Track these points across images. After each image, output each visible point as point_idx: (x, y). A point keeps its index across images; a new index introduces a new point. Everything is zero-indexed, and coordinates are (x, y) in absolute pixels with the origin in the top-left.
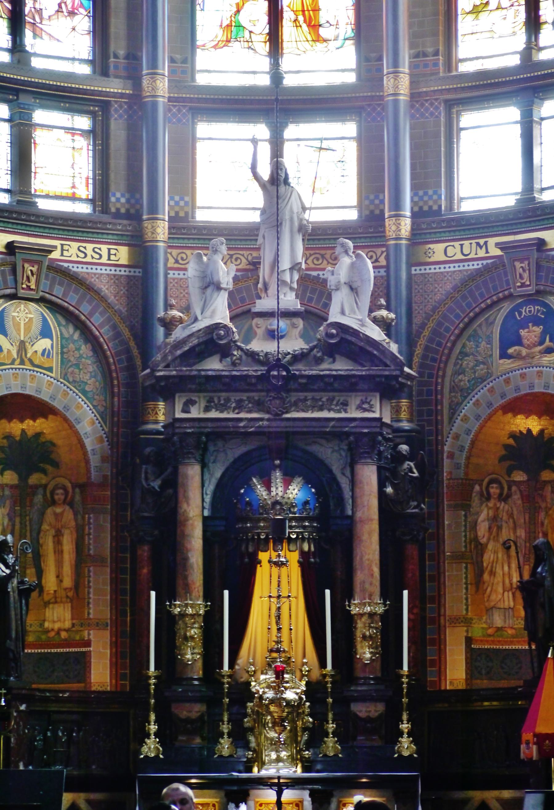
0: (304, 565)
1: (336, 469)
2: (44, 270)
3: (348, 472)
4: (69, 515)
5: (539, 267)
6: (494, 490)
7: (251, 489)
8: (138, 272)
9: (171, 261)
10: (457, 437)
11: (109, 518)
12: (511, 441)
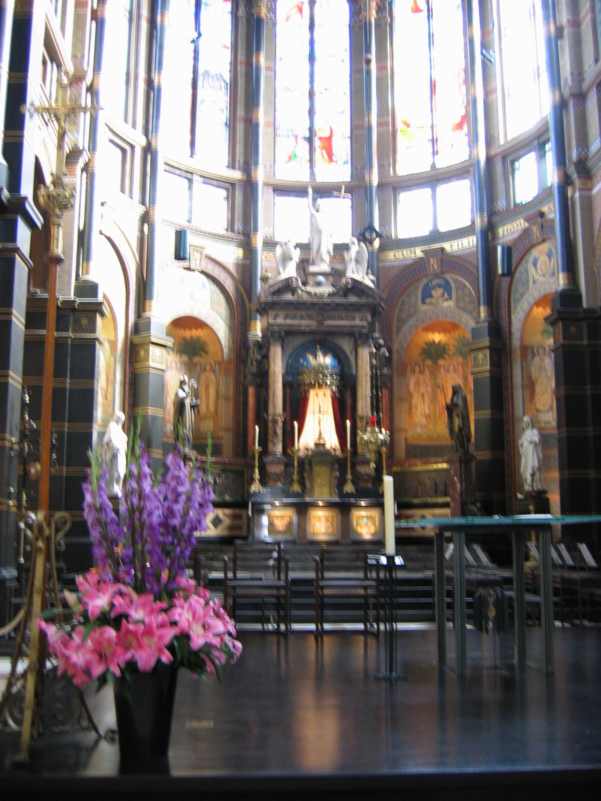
0: (334, 399)
1: (348, 352)
2: (204, 256)
3: (354, 354)
4: (212, 376)
5: (442, 261)
6: (417, 369)
7: (306, 360)
8: (248, 262)
9: (264, 258)
10: (400, 343)
11: (232, 379)
12: (426, 346)
